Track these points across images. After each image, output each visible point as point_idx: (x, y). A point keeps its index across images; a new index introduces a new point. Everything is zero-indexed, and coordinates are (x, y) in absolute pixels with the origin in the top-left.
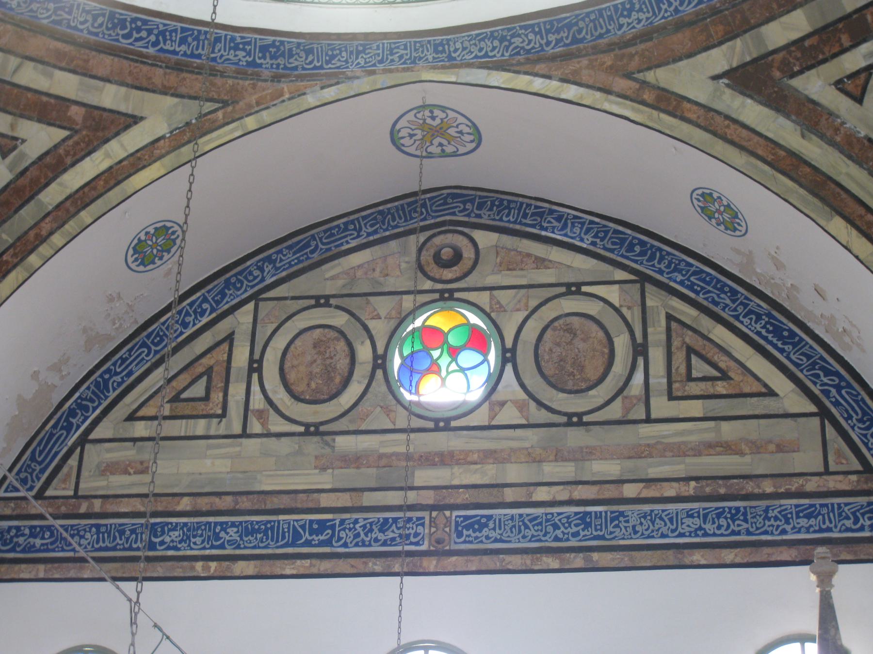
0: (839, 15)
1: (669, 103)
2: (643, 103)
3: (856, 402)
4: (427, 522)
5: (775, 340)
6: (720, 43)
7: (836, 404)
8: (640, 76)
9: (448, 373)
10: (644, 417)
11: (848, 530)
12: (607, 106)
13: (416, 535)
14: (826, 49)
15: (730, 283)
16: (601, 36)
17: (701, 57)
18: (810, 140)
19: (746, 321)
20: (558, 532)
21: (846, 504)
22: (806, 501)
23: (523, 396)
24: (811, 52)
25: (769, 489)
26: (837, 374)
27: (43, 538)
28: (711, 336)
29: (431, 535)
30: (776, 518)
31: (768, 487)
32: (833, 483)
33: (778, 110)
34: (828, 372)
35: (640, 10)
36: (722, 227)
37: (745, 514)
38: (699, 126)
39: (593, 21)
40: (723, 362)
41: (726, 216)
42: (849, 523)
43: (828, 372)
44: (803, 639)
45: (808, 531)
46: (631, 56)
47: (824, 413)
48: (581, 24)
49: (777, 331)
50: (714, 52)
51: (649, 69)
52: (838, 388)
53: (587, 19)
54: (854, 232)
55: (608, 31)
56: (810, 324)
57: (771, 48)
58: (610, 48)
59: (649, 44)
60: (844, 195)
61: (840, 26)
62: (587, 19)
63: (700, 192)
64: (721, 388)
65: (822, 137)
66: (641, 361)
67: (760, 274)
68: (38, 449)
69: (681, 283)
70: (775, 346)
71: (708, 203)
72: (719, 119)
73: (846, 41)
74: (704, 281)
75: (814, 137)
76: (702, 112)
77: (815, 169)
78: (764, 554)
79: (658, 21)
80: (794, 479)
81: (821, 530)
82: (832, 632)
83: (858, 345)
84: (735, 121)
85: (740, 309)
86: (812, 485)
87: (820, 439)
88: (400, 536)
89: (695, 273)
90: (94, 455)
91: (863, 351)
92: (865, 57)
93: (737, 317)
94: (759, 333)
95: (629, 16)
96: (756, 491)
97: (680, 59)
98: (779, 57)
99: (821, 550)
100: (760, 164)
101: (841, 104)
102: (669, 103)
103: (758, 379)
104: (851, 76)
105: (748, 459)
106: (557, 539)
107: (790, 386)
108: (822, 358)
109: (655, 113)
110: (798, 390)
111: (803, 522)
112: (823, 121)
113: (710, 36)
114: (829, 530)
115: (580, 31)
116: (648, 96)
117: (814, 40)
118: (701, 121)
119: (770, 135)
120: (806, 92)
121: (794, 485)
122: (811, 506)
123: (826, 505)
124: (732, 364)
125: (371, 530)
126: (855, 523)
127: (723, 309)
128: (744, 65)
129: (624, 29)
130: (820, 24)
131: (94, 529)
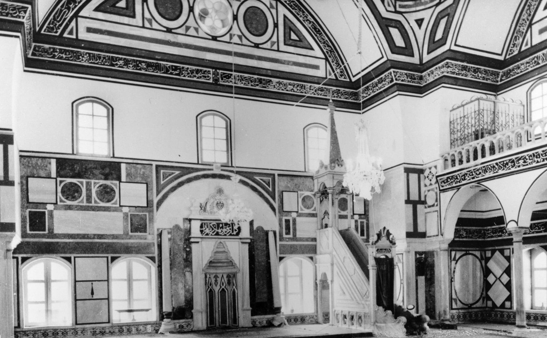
4: (211, 72)
9: (215, 19)
10: (276, 49)
13: (208, 77)
20: (252, 84)
23: (240, 34)
27: (66, 54)
29: (213, 78)
66: (276, 29)
68: (56, 16)
69: (288, 4)
88: (203, 76)
90: (83, 24)
93: (304, 21)
106: (252, 85)
125: (193, 73)
131: (88, 55)
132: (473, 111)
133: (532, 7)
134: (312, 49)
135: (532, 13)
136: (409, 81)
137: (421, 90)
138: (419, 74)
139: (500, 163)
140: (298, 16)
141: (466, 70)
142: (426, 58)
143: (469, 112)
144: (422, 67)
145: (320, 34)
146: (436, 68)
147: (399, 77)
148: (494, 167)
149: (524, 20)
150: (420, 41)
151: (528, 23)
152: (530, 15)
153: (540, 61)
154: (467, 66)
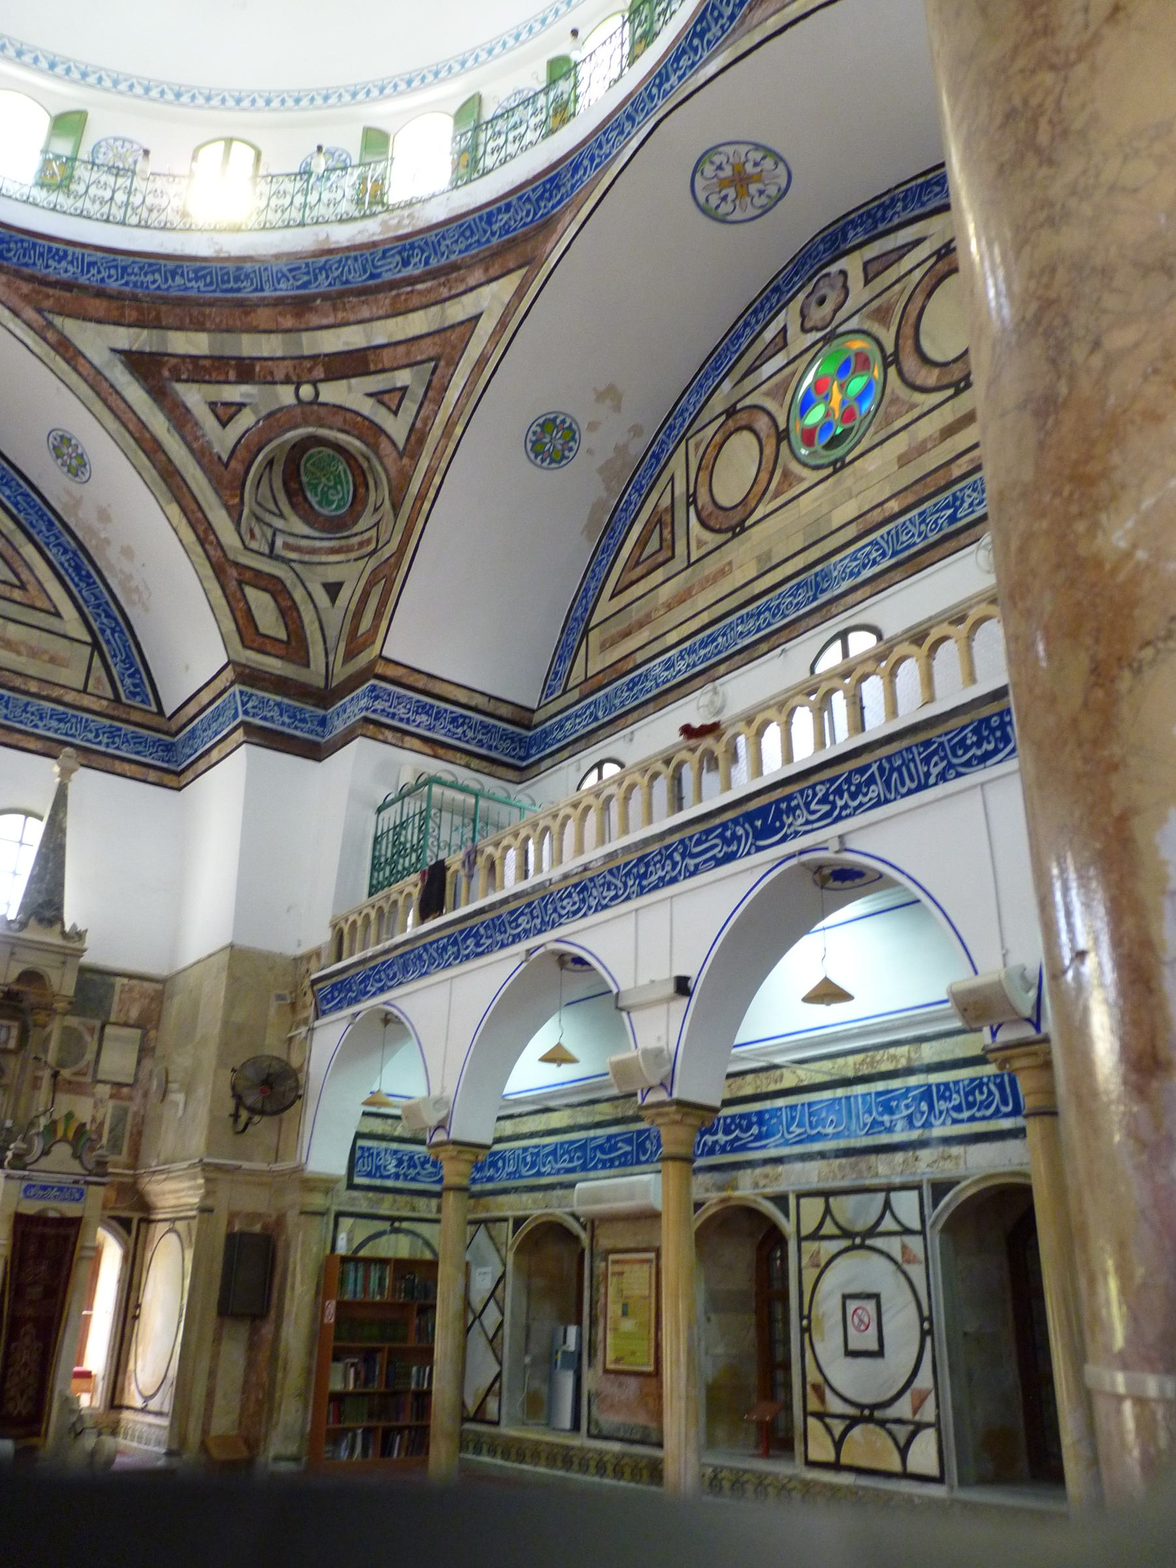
0: (235, 354)
1: (66, 349)
2: (45, 339)
3: (124, 647)
5: (73, 575)
6: (130, 326)
7: (108, 642)
8: (50, 316)
11: (88, 741)
12: (11, 326)
14: (214, 375)
15: (50, 514)
16: (26, 265)
17: (109, 329)
18: (173, 436)
19: (55, 550)
21: (93, 721)
22: (61, 708)
24: (202, 370)
25: (34, 689)
26: (115, 619)
28: (21, 550)
30: (33, 714)
31: (33, 687)
32: (87, 701)
33: (155, 400)
34: (109, 616)
35: (72, 262)
36: (65, 469)
37: (7, 702)
38: (86, 380)
39: (25, 249)
40: (25, 575)
41: (74, 462)
42: (91, 736)
43: (108, 616)
44: (28, 814)
45: (56, 731)
46: (47, 296)
47: (95, 645)
48: (12, 245)
49: (78, 568)
50: (122, 331)
51: (60, 314)
52: (113, 631)
53: (19, 245)
54: (184, 521)
55: (34, 264)
56: (106, 574)
57: (170, 351)
58: (31, 279)
59: (68, 295)
60: (185, 489)
61: (233, 362)
62: (19, 245)
63: (60, 433)
64: (17, 594)
65: (183, 438)
67: (82, 520)
69: (8, 498)
70: (72, 579)
71: (63, 447)
72: (104, 384)
73: (232, 375)
74: (28, 504)
75: (177, 436)
76: (92, 372)
77: (170, 461)
78: (15, 738)
79: (83, 280)
80: (57, 688)
81: (66, 734)
82: (61, 815)
83: (143, 604)
84: (118, 393)
85: (52, 539)
86: (70, 697)
87: (86, 663)
89: (21, 494)
91: (147, 610)
92: (242, 395)
93: (47, 544)
94: (62, 564)
95: (59, 262)
96: (23, 687)
97: (90, 320)
98: (173, 361)
99: (68, 750)
100: (127, 435)
101: (209, 422)
102: (66, 349)
103: (51, 600)
104: (225, 404)
105: (23, 659)
107: (76, 615)
108: (106, 603)
109: (52, 353)
110: (80, 621)
111: (54, 724)
112: (189, 426)
113: (122, 315)
114: (73, 736)
115: (9, 250)
116: (50, 335)
117: (207, 363)
118: (90, 379)
119: (143, 417)
120: (184, 399)
121: (56, 693)
122: (64, 713)
123: (77, 717)
124: (32, 580)
126: (97, 736)
127: (38, 533)
128: (141, 353)
129: (51, 270)
130: (217, 353)
132: (417, 811)
133: (590, 593)
134: (57, 614)
135: (590, 606)
136: (283, 724)
137: (315, 752)
138: (321, 712)
139: (431, 944)
140: (31, 530)
141: (427, 713)
142: (341, 672)
143: (411, 814)
144: (325, 696)
145: (91, 584)
146: (353, 699)
147: (254, 707)
148: (420, 957)
149: (576, 619)
150: (332, 633)
151: (582, 626)
152: (586, 610)
153: (600, 714)
154: (432, 706)
